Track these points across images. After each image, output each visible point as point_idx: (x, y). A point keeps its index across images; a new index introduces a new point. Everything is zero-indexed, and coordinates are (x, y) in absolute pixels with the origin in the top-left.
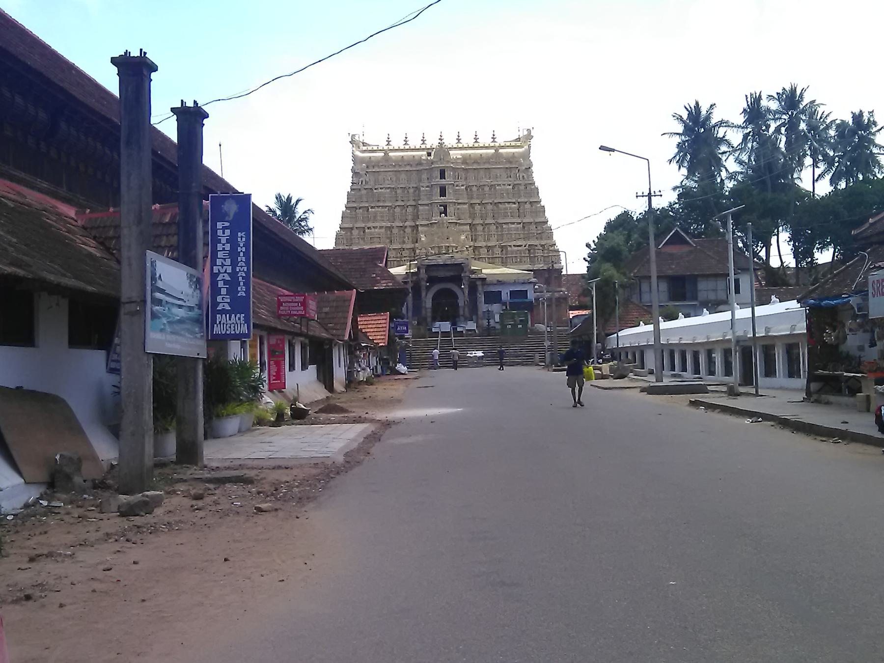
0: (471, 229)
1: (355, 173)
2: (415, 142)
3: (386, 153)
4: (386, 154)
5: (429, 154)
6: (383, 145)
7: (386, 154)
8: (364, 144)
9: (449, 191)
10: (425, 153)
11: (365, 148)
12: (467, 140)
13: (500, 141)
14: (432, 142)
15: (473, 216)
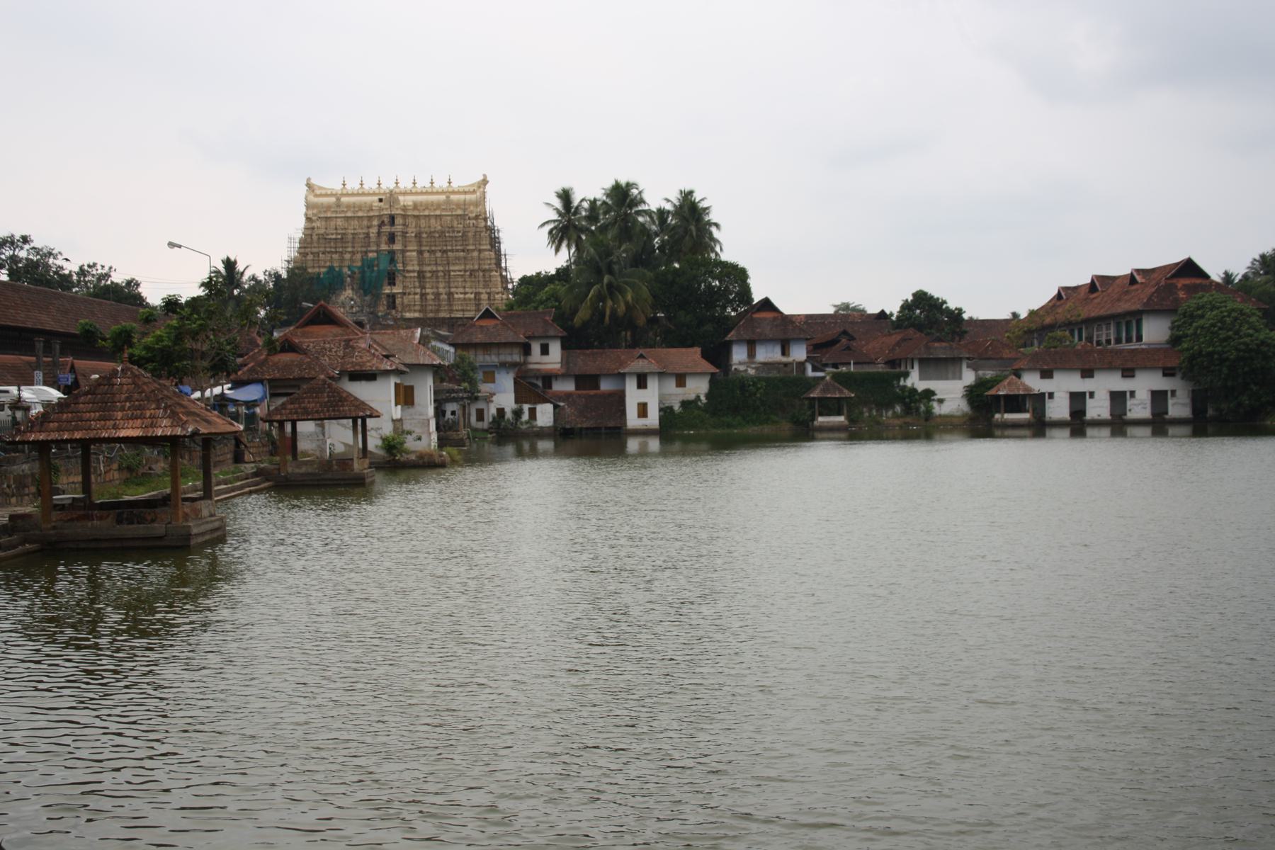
0: (419, 277)
1: (308, 219)
2: (371, 185)
3: (338, 197)
4: (338, 199)
5: (381, 200)
6: (337, 187)
7: (338, 199)
8: (321, 188)
9: (399, 238)
10: (376, 198)
11: (318, 192)
12: (423, 183)
13: (455, 185)
14: (388, 185)
15: (421, 263)
